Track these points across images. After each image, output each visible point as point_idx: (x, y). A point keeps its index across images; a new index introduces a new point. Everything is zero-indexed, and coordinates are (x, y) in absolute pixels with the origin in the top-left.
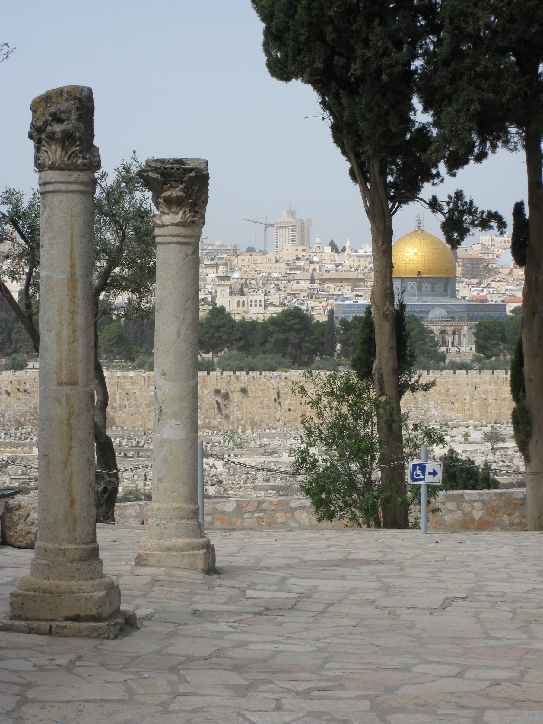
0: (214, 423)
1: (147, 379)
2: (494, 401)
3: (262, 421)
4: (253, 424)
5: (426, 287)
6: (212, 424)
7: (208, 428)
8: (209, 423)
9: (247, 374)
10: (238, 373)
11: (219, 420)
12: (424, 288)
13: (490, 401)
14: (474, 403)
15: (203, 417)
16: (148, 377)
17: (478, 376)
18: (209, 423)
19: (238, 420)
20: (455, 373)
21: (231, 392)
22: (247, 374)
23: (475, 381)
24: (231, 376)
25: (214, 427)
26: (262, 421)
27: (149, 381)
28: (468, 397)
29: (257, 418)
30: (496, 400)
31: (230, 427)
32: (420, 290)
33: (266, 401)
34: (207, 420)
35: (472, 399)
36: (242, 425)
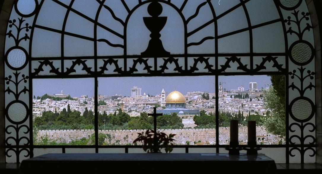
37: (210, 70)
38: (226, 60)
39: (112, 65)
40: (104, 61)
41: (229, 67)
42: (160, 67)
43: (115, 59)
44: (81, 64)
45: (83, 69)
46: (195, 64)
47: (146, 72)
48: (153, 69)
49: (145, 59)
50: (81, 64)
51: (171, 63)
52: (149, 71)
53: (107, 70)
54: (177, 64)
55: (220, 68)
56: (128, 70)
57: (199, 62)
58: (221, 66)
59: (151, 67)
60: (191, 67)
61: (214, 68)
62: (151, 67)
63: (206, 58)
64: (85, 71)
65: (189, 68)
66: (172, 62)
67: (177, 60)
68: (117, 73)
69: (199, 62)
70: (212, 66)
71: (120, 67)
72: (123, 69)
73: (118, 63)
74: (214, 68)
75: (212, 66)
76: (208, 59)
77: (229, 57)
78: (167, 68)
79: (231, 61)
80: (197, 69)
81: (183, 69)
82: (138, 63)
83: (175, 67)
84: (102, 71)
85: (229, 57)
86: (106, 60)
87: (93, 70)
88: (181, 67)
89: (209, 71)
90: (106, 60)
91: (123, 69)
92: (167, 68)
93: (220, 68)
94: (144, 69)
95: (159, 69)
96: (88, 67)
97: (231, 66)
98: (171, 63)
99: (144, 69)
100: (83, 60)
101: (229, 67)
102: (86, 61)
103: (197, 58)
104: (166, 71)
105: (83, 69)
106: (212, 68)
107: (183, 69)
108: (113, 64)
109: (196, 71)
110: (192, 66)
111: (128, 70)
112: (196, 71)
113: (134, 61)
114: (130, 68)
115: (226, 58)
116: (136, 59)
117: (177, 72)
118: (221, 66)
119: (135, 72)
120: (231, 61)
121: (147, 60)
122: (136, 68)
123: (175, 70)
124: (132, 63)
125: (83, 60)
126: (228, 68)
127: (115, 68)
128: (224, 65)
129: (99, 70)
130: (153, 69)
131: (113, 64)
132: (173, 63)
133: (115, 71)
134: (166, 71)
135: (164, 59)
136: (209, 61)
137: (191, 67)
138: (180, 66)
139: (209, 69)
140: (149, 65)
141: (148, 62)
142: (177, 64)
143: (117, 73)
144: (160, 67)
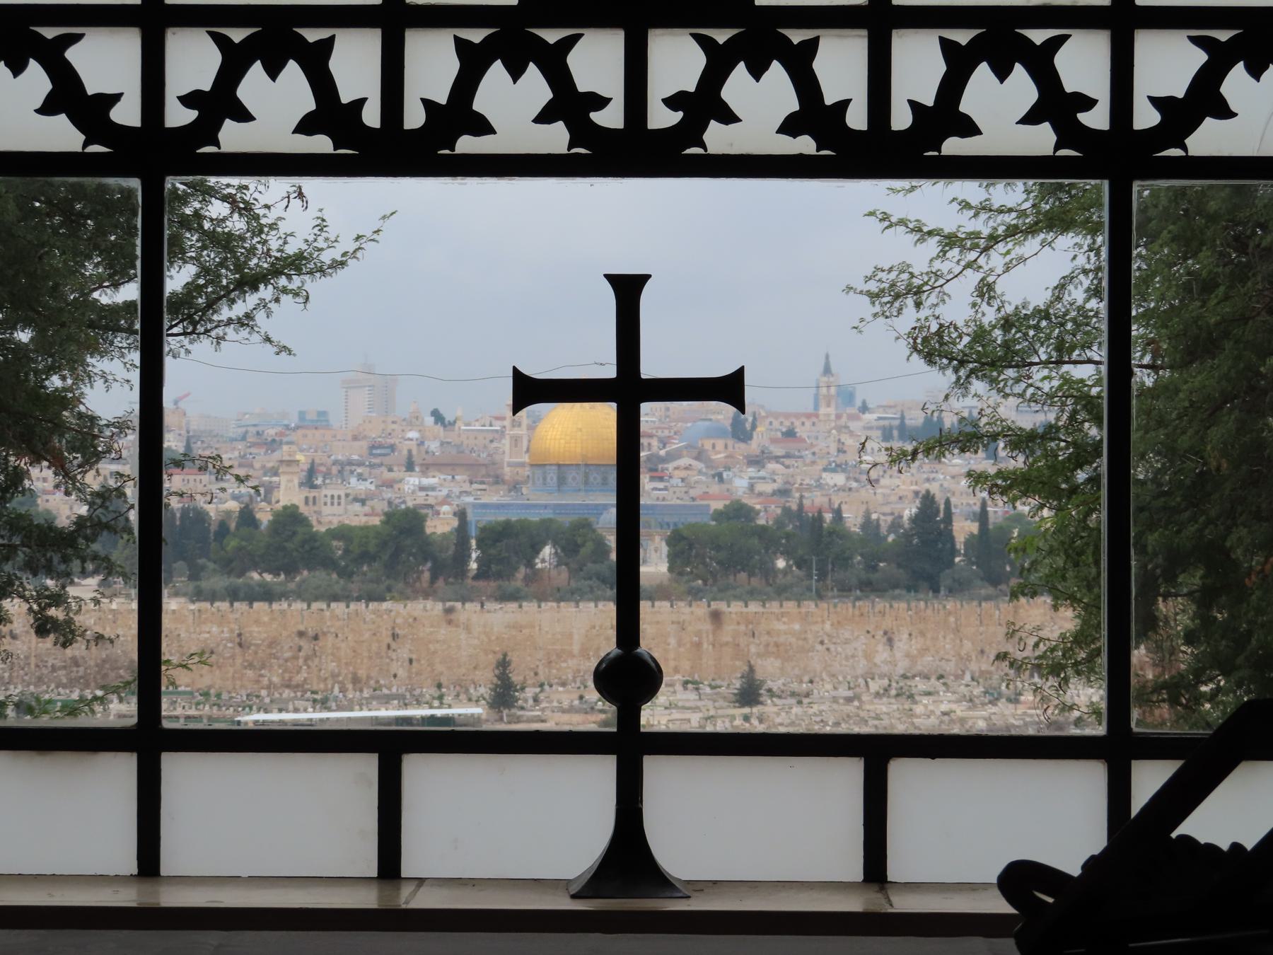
0: (299, 678)
1: (197, 614)
2: (711, 647)
3: (369, 677)
4: (356, 680)
5: (595, 478)
6: (293, 683)
7: (288, 686)
8: (290, 680)
9: (348, 607)
10: (333, 605)
11: (305, 675)
12: (591, 479)
13: (705, 646)
14: (682, 650)
15: (280, 671)
16: (199, 611)
17: (688, 610)
18: (290, 680)
19: (334, 676)
20: (653, 606)
21: (325, 634)
22: (348, 607)
23: (683, 617)
24: (322, 610)
25: (297, 686)
26: (369, 677)
27: (200, 617)
28: (672, 641)
29: (362, 673)
30: (714, 646)
31: (322, 686)
32: (586, 483)
33: (374, 647)
34: (287, 676)
35: (680, 644)
36: (339, 682)
37: (1069, 132)
38: (1200, 57)
39: (282, 76)
40: (221, 41)
41: (1223, 111)
42: (673, 102)
43: (312, 35)
44: (34, 69)
45: (48, 108)
46: (952, 86)
47: (556, 138)
48: (611, 118)
49: (552, 36)
50: (34, 69)
51: (757, 72)
52: (582, 130)
53: (243, 115)
54: (806, 84)
55: (1145, 117)
56: (414, 118)
57: (983, 73)
58: (1155, 101)
59: (600, 102)
60: (914, 105)
61: (1097, 119)
62: (600, 102)
63: (1038, 36)
64: (62, 118)
65: (901, 119)
66: (765, 67)
67: (811, 47)
68: (321, 144)
69: (983, 73)
70: (1087, 103)
71: (346, 97)
72: (372, 116)
73: (338, 65)
74: (1097, 119)
75: (1087, 103)
76: (1058, 43)
77: (1223, 36)
78: (728, 117)
79: (1239, 71)
80: (968, 128)
81: (857, 119)
82: (497, 70)
83: (790, 103)
84: (206, 129)
85: (1223, 36)
86: (237, 35)
87: (127, 114)
88: (843, 105)
89: (1057, 148)
90: (237, 35)
91: (372, 116)
92: (728, 117)
93: (1145, 117)
94: (545, 117)
95: (661, 118)
96: (93, 85)
97: (1233, 108)
98: (757, 72)
99: (545, 117)
100: (49, 33)
101: (1223, 111)
102: (78, 38)
103: (963, 37)
104: (718, 138)
105: (48, 108)
106: (1086, 118)
107: (857, 119)
108: (292, 70)
109: (953, 146)
110: (928, 100)
111: (414, 118)
112: (953, 146)
113: (461, 45)
114: (428, 104)
115: (1195, 40)
116: (476, 36)
117: (805, 145)
118: (1155, 101)
119: (467, 144)
120: (1239, 71)
121: (569, 43)
122: (479, 105)
123: (790, 127)
124: (452, 66)
125: (49, 33)
126: (1210, 124)
127: (310, 105)
128: (1180, 93)
129: (178, 116)
130: (611, 118)
131: (292, 70)
132: (776, 67)
133: (306, 126)
134: (718, 138)
135: (705, 43)
136: (1062, 60)
137: (912, 103)
138: (829, 99)
139: (1056, 129)
140: (582, 86)
141: (575, 60)
142: (806, 84)
143: (321, 144)
144: (673, 102)
